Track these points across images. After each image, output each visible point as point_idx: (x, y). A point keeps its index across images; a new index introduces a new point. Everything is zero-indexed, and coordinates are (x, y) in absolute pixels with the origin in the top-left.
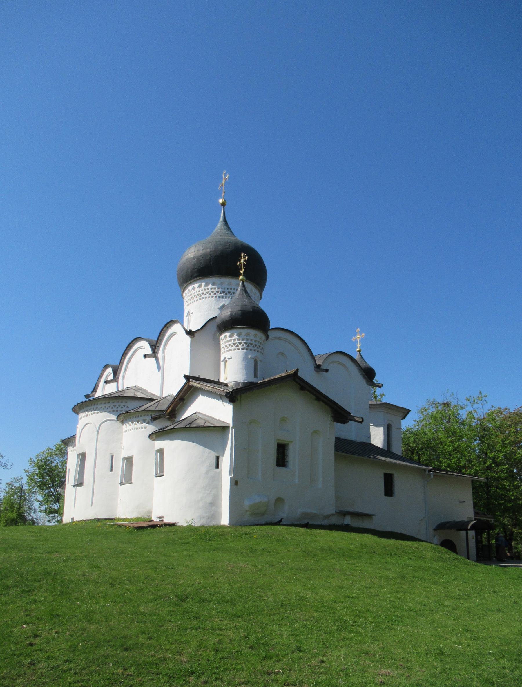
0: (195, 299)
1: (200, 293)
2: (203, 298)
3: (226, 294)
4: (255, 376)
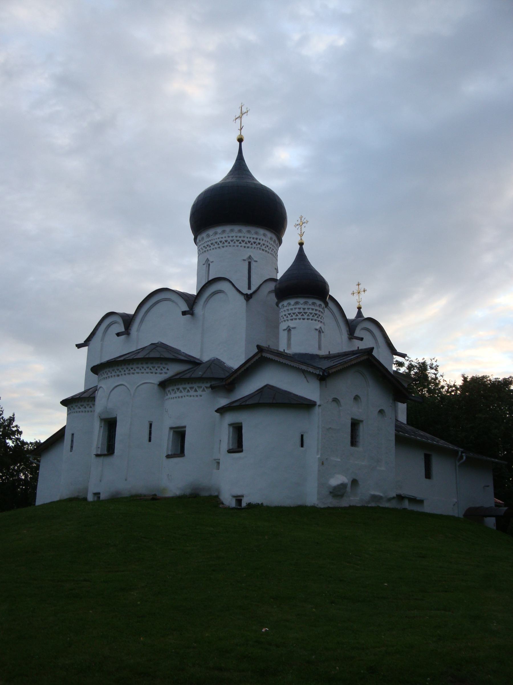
0: (216, 246)
1: (223, 240)
2: (227, 246)
3: (252, 244)
4: (320, 348)
